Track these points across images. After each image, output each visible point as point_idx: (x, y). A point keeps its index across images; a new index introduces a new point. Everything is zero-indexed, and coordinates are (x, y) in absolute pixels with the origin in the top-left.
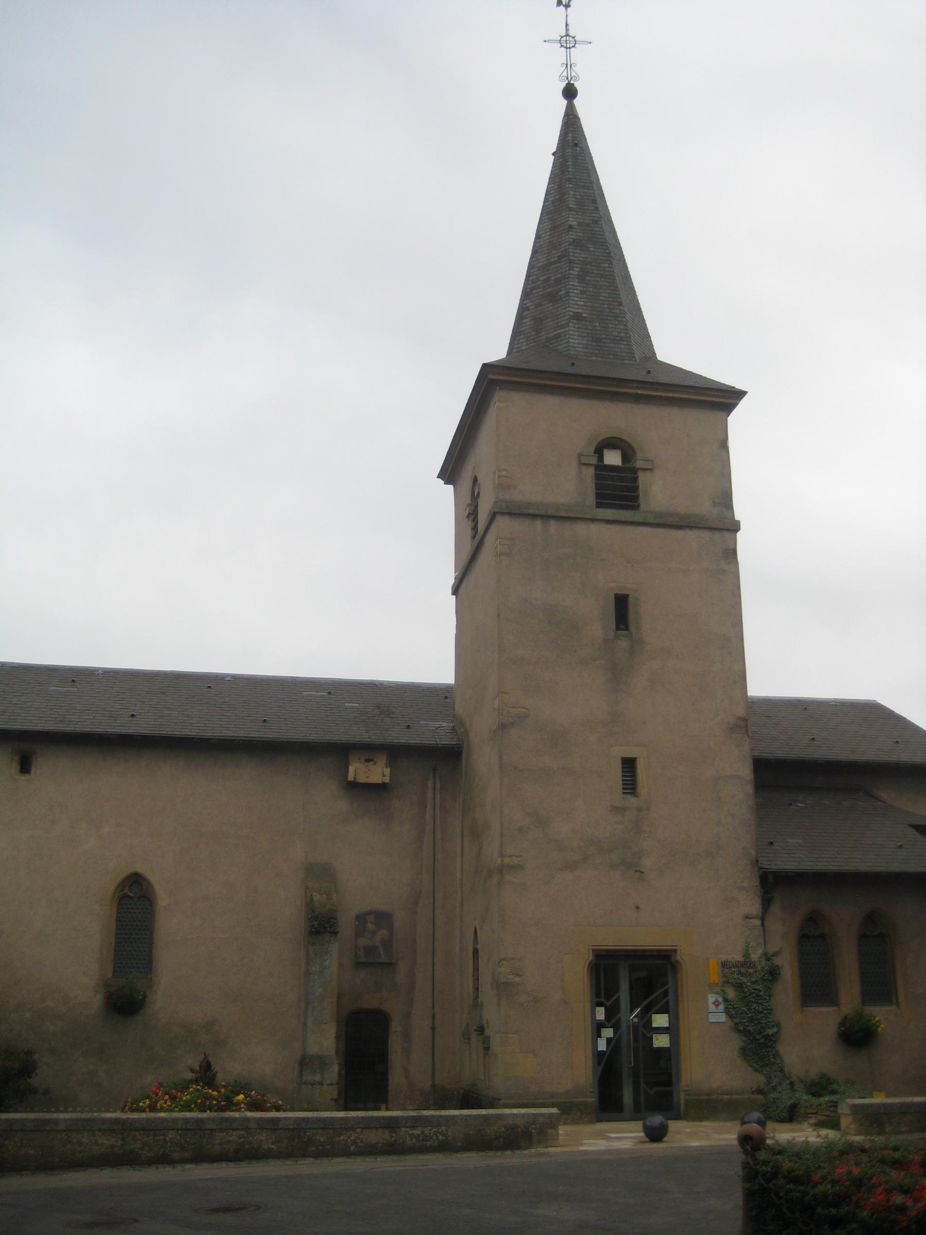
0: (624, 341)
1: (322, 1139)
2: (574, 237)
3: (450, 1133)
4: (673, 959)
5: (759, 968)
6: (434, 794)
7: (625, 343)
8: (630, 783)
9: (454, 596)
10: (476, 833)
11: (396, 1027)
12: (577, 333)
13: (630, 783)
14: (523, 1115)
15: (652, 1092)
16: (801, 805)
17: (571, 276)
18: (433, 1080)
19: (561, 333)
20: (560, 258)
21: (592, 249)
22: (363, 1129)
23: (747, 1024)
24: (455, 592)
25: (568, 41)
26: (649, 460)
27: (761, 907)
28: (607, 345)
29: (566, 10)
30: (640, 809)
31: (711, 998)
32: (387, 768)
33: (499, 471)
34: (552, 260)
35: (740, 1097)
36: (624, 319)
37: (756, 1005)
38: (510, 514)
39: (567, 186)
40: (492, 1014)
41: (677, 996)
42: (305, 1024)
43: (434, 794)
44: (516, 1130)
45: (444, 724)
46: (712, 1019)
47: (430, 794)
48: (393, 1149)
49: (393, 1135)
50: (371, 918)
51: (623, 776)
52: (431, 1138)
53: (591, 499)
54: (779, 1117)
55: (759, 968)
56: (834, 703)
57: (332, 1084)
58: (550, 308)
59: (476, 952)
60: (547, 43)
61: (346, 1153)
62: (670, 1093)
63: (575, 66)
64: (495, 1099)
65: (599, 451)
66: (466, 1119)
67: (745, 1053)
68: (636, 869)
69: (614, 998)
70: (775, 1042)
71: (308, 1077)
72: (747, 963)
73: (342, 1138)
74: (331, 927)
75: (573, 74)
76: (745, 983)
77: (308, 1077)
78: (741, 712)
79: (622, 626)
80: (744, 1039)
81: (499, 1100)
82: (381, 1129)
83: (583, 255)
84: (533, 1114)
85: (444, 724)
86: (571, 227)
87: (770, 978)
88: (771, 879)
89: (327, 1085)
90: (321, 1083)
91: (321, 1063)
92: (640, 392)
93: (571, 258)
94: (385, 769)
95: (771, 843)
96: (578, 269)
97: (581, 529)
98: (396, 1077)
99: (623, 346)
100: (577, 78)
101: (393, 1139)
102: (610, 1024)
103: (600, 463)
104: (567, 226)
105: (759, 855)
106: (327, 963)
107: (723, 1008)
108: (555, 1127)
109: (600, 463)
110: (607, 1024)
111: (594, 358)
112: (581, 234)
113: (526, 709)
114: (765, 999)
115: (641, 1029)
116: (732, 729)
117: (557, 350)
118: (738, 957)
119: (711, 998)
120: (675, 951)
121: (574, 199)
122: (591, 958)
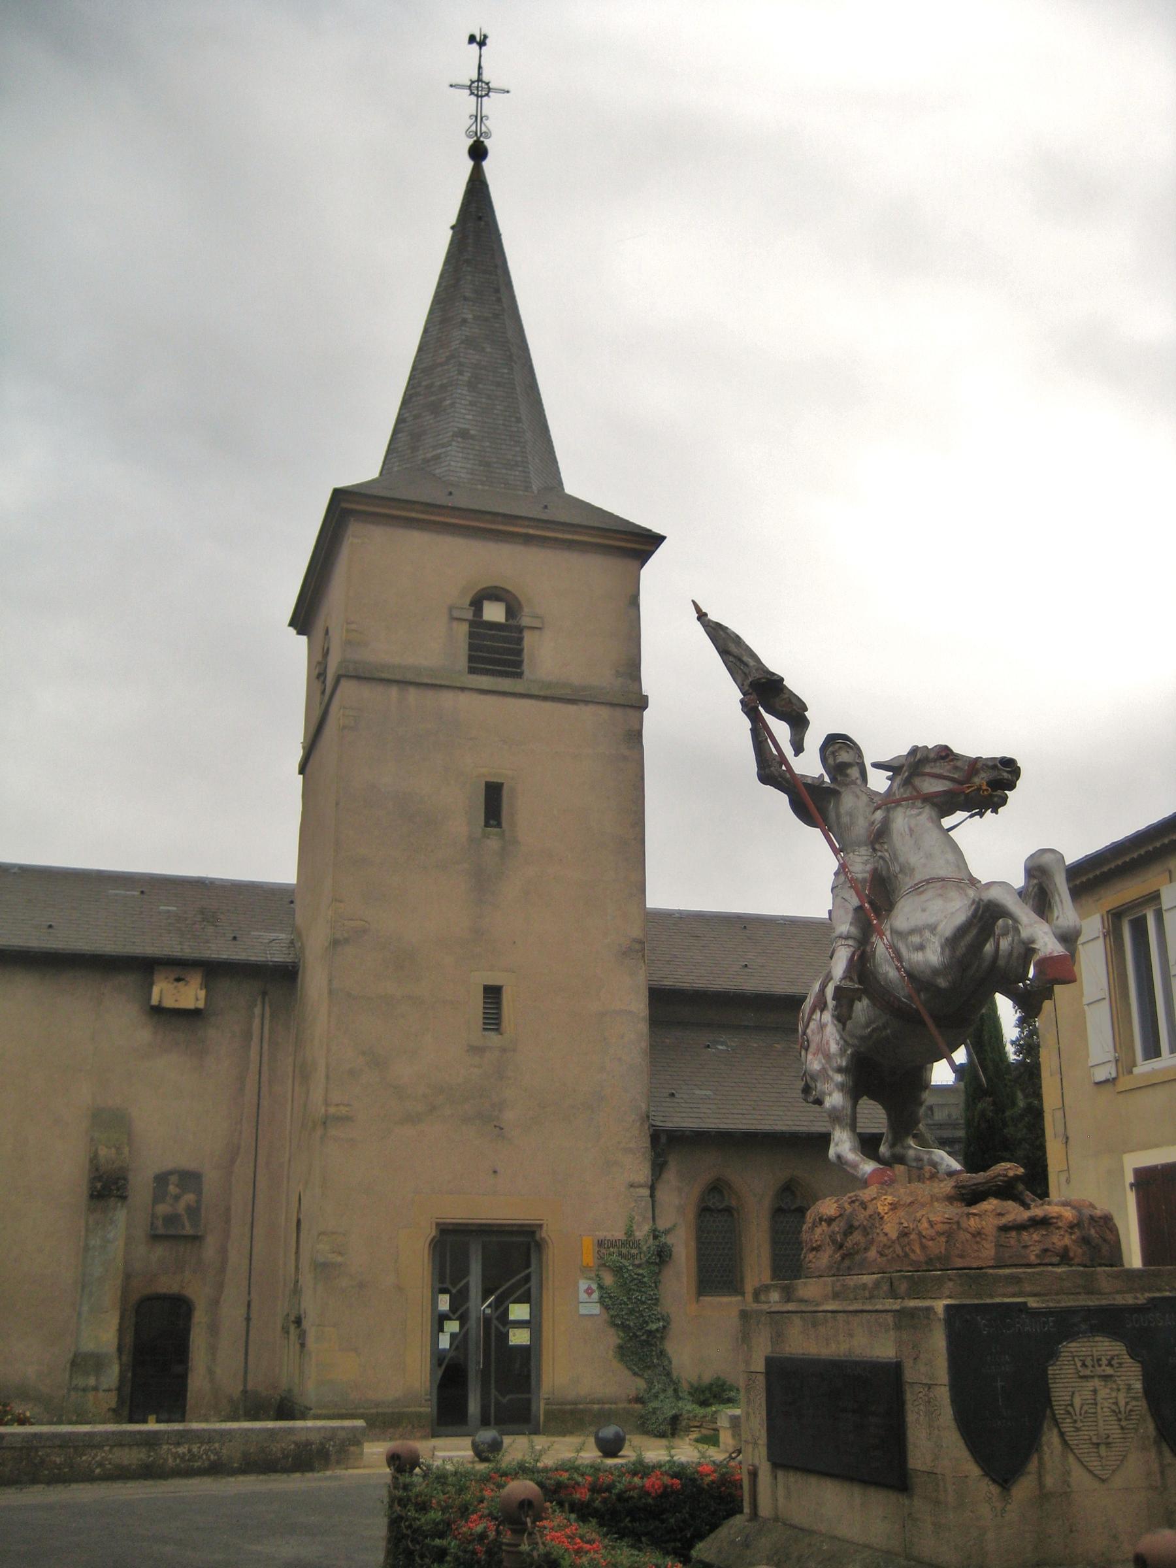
0: (519, 466)
1: (58, 1460)
2: (468, 334)
3: (224, 1451)
4: (537, 1237)
5: (645, 1248)
6: (262, 1024)
7: (520, 469)
8: (493, 1017)
9: (301, 776)
10: (304, 1074)
11: (200, 1317)
12: (460, 455)
13: (493, 1017)
14: (319, 1429)
15: (505, 1400)
16: (720, 1047)
17: (459, 382)
18: (245, 1386)
19: (441, 453)
20: (449, 358)
21: (488, 350)
22: (112, 1447)
23: (626, 1317)
24: (302, 770)
25: (479, 88)
26: (537, 617)
27: (650, 1173)
28: (498, 471)
29: (480, 48)
30: (504, 1050)
31: (583, 1285)
32: (201, 989)
33: (348, 623)
34: (438, 361)
35: (613, 1406)
36: (523, 440)
37: (638, 1294)
38: (358, 678)
39: (464, 269)
40: (310, 1304)
41: (541, 1280)
42: (79, 1314)
43: (262, 1024)
44: (309, 1447)
45: (283, 936)
46: (583, 1310)
47: (256, 1022)
48: (149, 1472)
49: (152, 1454)
50: (174, 1179)
51: (484, 1008)
52: (200, 1457)
53: (463, 663)
54: (658, 1431)
55: (645, 1248)
56: (782, 922)
57: (109, 1390)
58: (431, 421)
59: (299, 1222)
60: (453, 89)
61: (88, 1477)
62: (529, 1401)
63: (487, 120)
64: (306, 1408)
65: (477, 604)
66: (246, 1434)
67: (622, 1352)
68: (495, 1123)
69: (462, 1283)
70: (662, 1338)
71: (80, 1381)
72: (630, 1241)
73: (84, 1458)
74: (118, 1189)
75: (484, 129)
76: (625, 1266)
77: (80, 1381)
78: (636, 933)
79: (492, 822)
80: (622, 1334)
81: (311, 1409)
82: (135, 1447)
83: (477, 357)
84: (331, 1427)
85: (283, 936)
86: (464, 321)
87: (657, 1261)
88: (663, 1139)
89: (104, 1391)
90: (96, 1389)
91: (96, 1363)
92: (531, 531)
93: (462, 360)
94: (199, 991)
95: (673, 1095)
96: (469, 375)
97: (447, 699)
98: (197, 1382)
99: (517, 473)
100: (488, 135)
101: (151, 1459)
102: (456, 1315)
103: (478, 619)
104: (460, 320)
105: (653, 1109)
106: (111, 1236)
107: (597, 1298)
108: (358, 1443)
109: (478, 619)
110: (451, 1315)
111: (480, 487)
112: (477, 330)
113: (366, 922)
114: (650, 1287)
115: (495, 1322)
116: (626, 953)
117: (434, 475)
118: (619, 1235)
119: (583, 1285)
120: (541, 1226)
121: (471, 286)
122: (434, 1233)
